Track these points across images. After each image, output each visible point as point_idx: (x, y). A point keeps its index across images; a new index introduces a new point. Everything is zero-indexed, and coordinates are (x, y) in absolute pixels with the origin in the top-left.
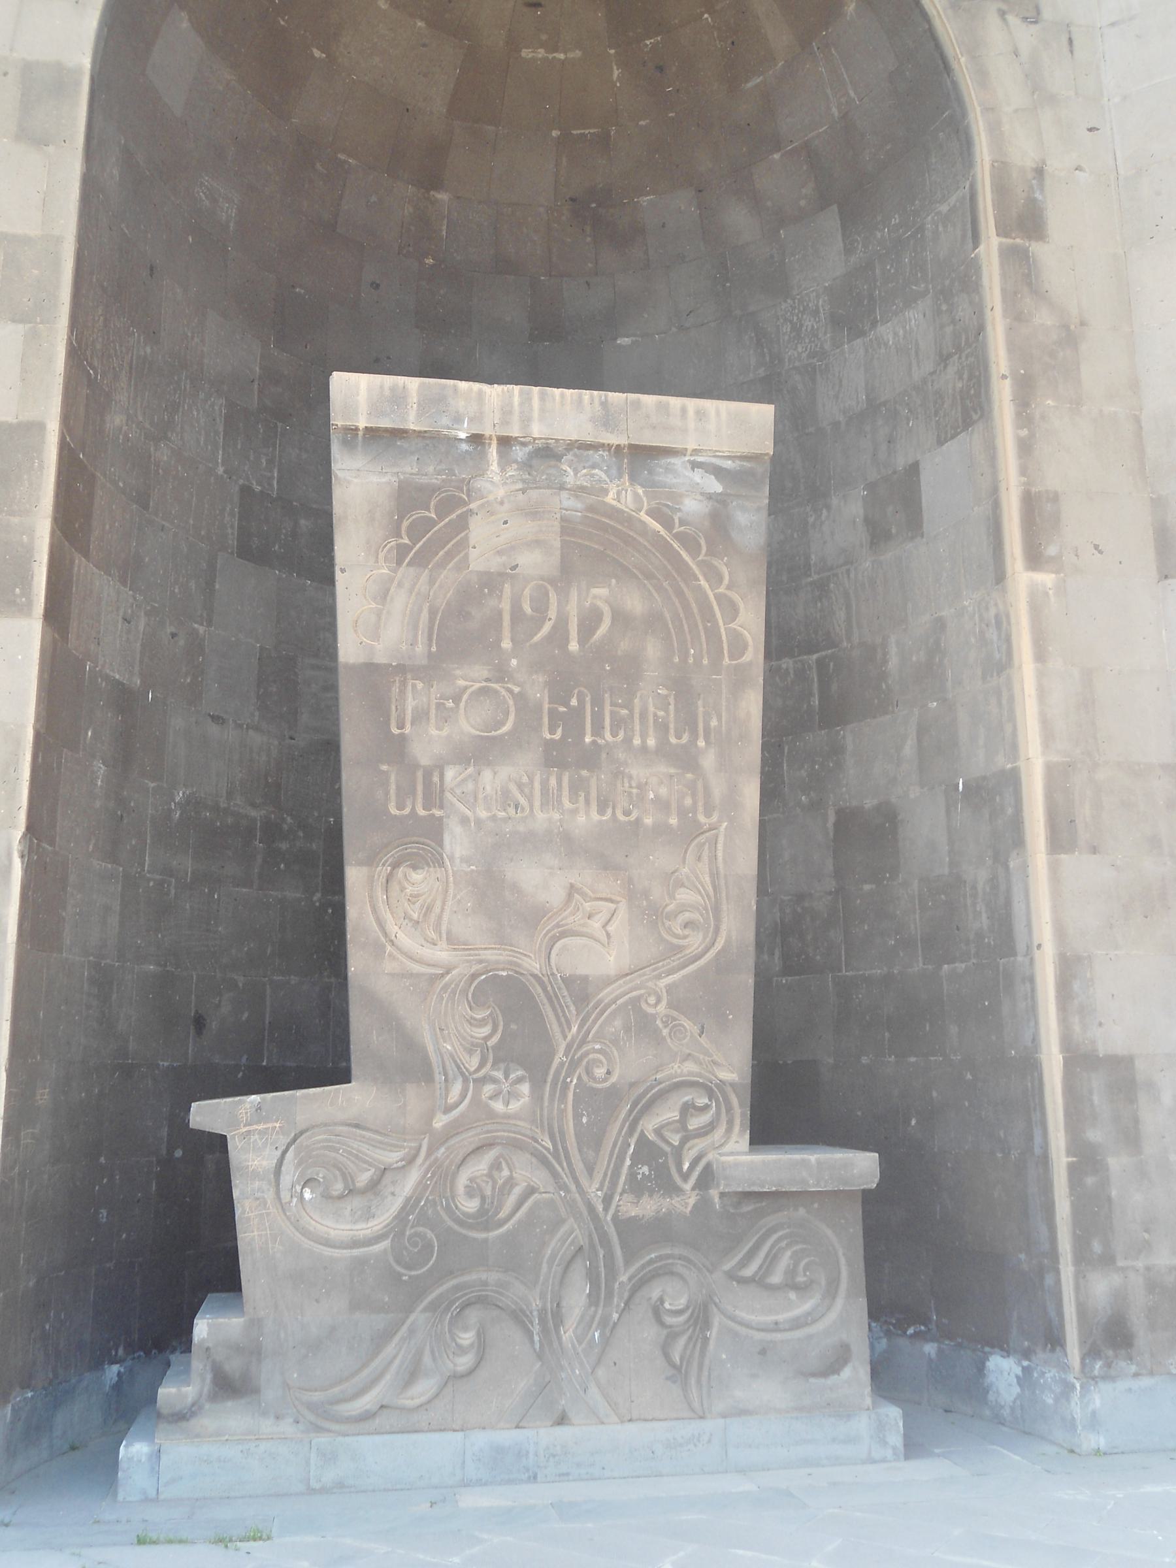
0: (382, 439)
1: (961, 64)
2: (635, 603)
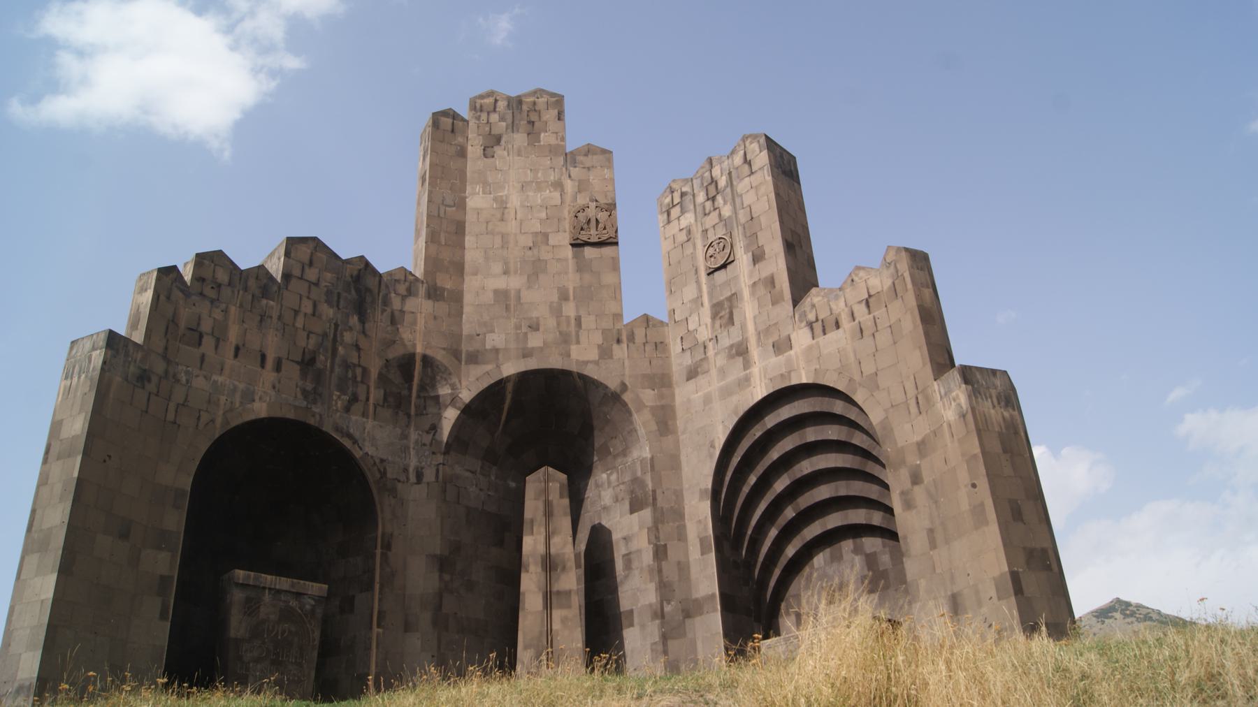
0: (244, 586)
1: (378, 507)
2: (293, 629)
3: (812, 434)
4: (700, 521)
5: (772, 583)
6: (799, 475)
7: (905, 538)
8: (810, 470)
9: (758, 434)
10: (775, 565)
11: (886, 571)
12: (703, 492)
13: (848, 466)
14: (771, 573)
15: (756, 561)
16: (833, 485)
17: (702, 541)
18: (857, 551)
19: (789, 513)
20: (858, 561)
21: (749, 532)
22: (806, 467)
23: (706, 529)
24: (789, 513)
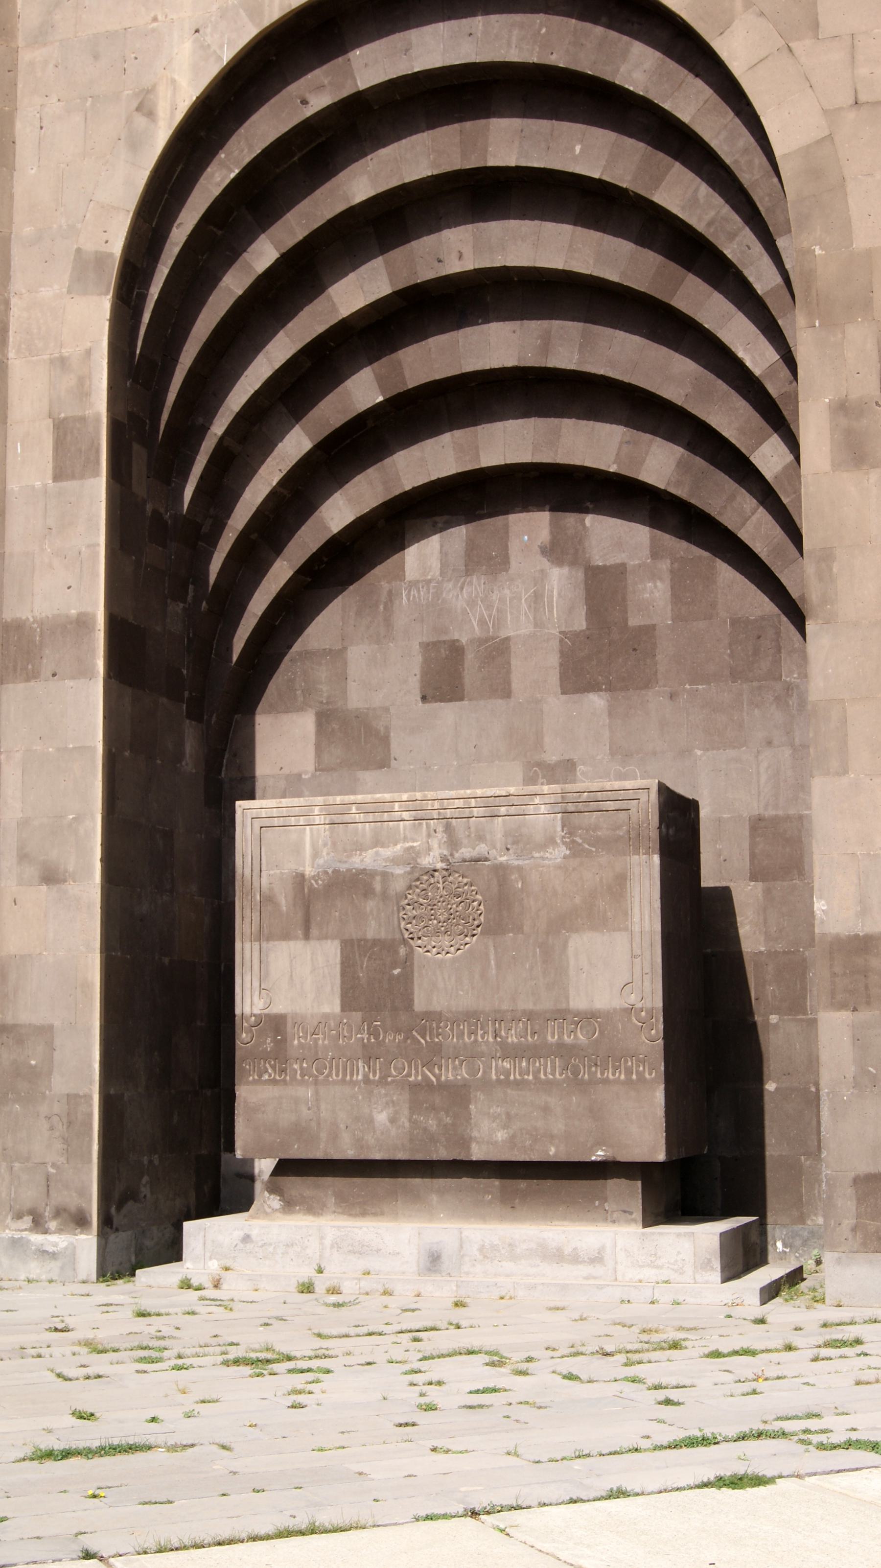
3: (509, 142)
4: (63, 363)
5: (259, 603)
6: (426, 273)
7: (827, 556)
8: (469, 264)
9: (319, 102)
10: (278, 549)
11: (649, 630)
12: (85, 265)
13: (613, 276)
14: (260, 571)
15: (219, 526)
16: (535, 326)
17: (64, 432)
18: (557, 551)
19: (363, 390)
20: (560, 581)
21: (219, 427)
22: (459, 249)
23: (83, 392)
24: (363, 390)
